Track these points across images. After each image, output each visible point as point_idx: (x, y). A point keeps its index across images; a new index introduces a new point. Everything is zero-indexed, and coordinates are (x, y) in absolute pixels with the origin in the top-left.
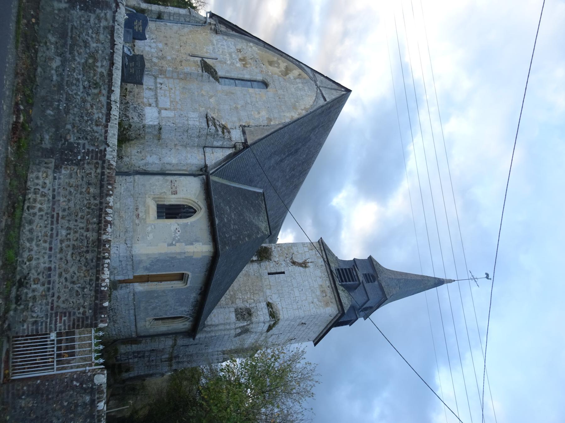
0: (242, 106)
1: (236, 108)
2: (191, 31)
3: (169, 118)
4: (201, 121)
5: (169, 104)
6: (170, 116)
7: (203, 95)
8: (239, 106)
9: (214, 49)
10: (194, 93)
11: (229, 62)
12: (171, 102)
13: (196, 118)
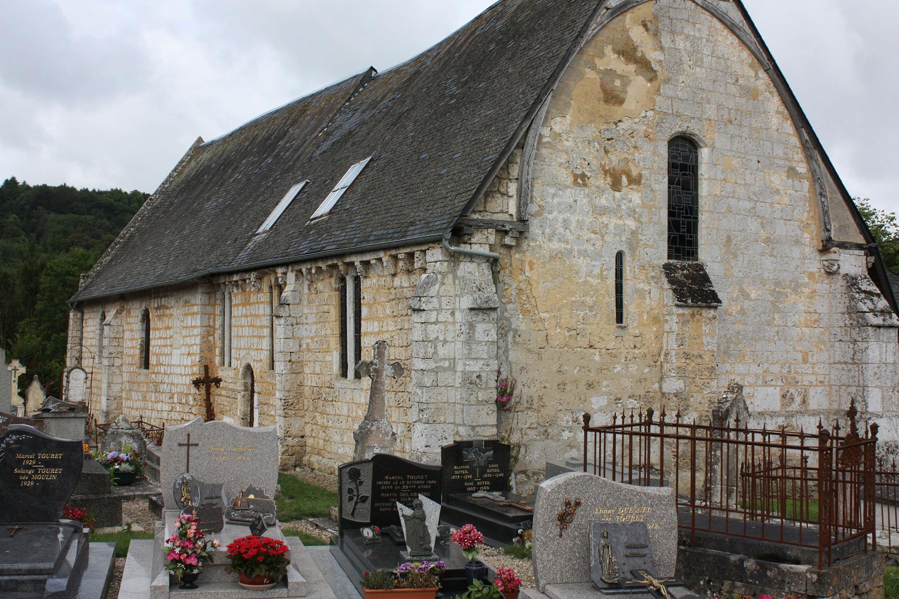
0: (763, 225)
1: (768, 241)
2: (525, 312)
3: (883, 398)
4: (885, 339)
5: (770, 390)
6: (880, 396)
7: (742, 312)
8: (763, 234)
9: (584, 253)
10: (738, 333)
11: (631, 224)
12: (765, 384)
13: (881, 347)
